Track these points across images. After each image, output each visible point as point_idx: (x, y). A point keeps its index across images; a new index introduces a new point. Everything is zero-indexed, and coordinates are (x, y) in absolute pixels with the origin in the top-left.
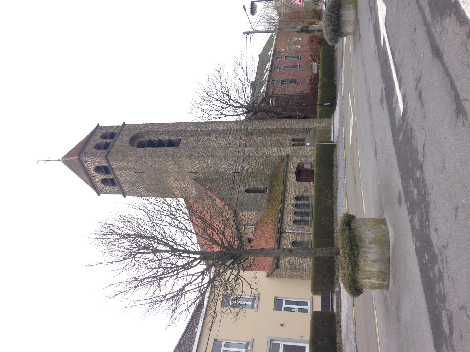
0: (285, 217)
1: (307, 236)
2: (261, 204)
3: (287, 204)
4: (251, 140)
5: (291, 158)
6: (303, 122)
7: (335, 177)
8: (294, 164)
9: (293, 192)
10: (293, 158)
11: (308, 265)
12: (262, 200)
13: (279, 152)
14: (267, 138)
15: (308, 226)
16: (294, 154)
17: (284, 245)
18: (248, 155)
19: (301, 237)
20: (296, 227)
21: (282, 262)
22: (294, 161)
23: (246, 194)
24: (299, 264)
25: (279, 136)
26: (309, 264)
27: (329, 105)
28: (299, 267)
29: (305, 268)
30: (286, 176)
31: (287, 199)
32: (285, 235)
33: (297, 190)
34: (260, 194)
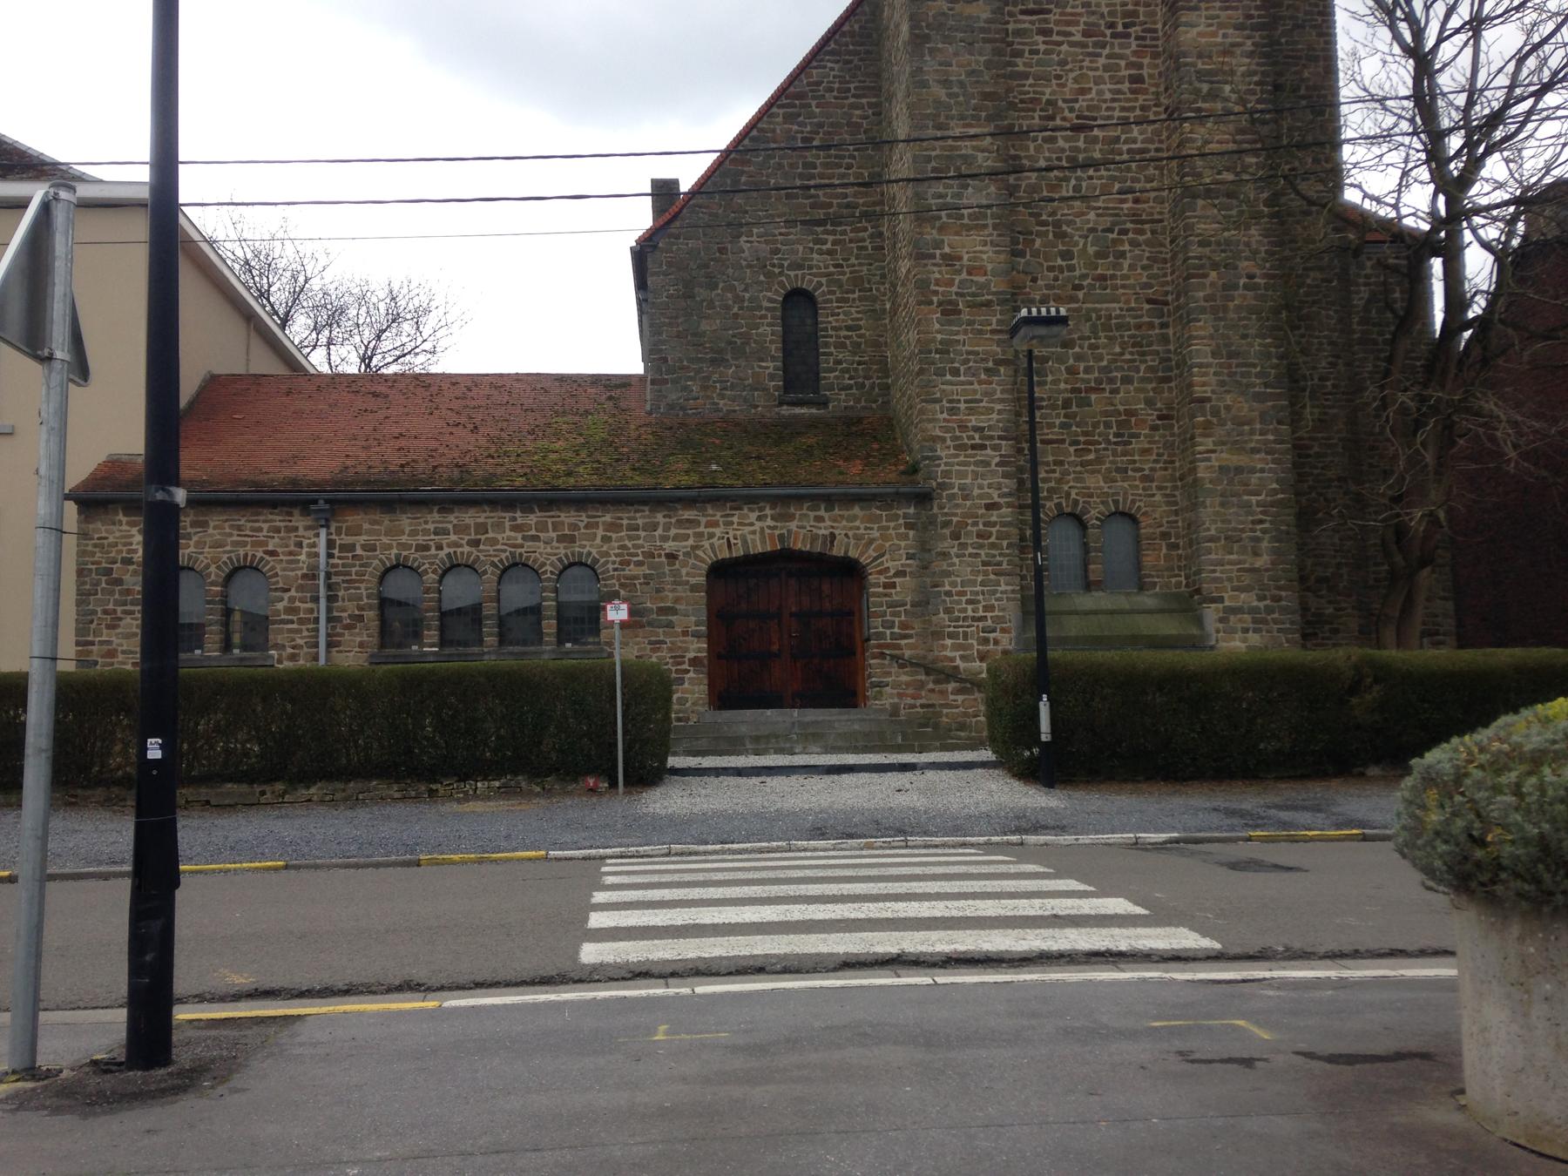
0: (432, 519)
1: (300, 642)
2: (704, 388)
3: (532, 519)
4: (1122, 255)
5: (906, 516)
6: (1263, 561)
7: (312, 790)
8: (858, 538)
9: (623, 547)
10: (909, 526)
11: (111, 654)
12: (733, 387)
13: (955, 438)
14: (1143, 354)
15: (375, 640)
16: (947, 532)
17: (231, 527)
18: (933, 256)
19: (291, 610)
20: (362, 581)
21: (125, 527)
22: (884, 538)
23: (771, 297)
24: (115, 611)
25: (1154, 428)
26: (121, 657)
27: (1039, 733)
28: (99, 609)
29: (92, 643)
30: (752, 500)
31: (567, 517)
32: (307, 528)
33: (645, 570)
34: (772, 377)
